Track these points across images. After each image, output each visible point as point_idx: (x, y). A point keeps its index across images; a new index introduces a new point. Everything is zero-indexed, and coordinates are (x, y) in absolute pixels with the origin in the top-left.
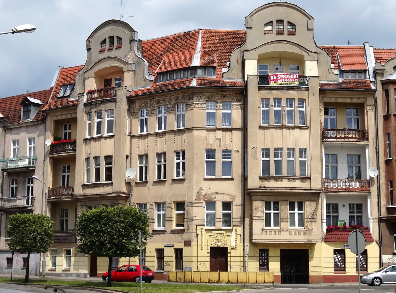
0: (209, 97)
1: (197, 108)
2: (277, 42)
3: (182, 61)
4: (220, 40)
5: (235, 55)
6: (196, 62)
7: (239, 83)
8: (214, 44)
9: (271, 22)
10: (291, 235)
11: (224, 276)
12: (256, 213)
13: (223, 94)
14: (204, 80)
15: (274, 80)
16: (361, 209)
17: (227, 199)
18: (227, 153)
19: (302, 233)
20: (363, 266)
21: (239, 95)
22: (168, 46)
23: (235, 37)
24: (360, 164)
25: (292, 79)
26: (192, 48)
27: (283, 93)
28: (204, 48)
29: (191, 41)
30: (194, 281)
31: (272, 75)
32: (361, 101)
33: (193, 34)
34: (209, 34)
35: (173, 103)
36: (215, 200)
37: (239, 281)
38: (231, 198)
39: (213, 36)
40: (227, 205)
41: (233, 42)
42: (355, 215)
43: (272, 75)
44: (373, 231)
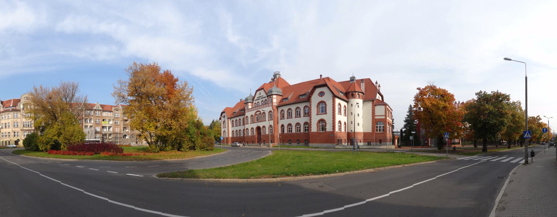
5: (19, 104)
6: (11, 106)
11: (17, 146)
17: (18, 131)
18: (17, 123)
26: (11, 103)
28: (13, 103)
34: (14, 100)
40: (18, 133)
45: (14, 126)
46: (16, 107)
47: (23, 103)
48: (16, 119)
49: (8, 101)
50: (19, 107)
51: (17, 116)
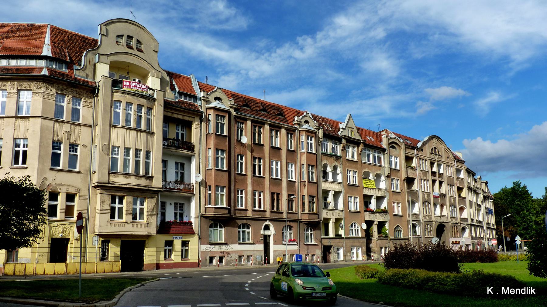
0: (59, 90)
1: (46, 98)
2: (128, 54)
3: (29, 48)
4: (69, 39)
7: (91, 82)
8: (64, 41)
9: (122, 36)
10: (134, 227)
12: (103, 206)
13: (74, 89)
14: (56, 72)
15: (127, 86)
16: (182, 207)
17: (72, 191)
18: (73, 147)
19: (143, 226)
20: (184, 254)
21: (89, 93)
22: (8, 32)
23: (84, 41)
24: (183, 170)
25: (143, 89)
27: (134, 98)
29: (38, 33)
30: (37, 273)
31: (125, 81)
32: (190, 119)
33: (40, 27)
35: (16, 88)
36: (59, 191)
37: (87, 272)
38: (76, 190)
39: (62, 34)
40: (70, 197)
41: (82, 45)
42: (178, 212)
43: (125, 81)
44: (195, 225)
45: (56, 159)
46: (70, 66)
47: (111, 58)
48: (67, 127)
49: (19, 28)
50: (89, 71)
51: (75, 113)
